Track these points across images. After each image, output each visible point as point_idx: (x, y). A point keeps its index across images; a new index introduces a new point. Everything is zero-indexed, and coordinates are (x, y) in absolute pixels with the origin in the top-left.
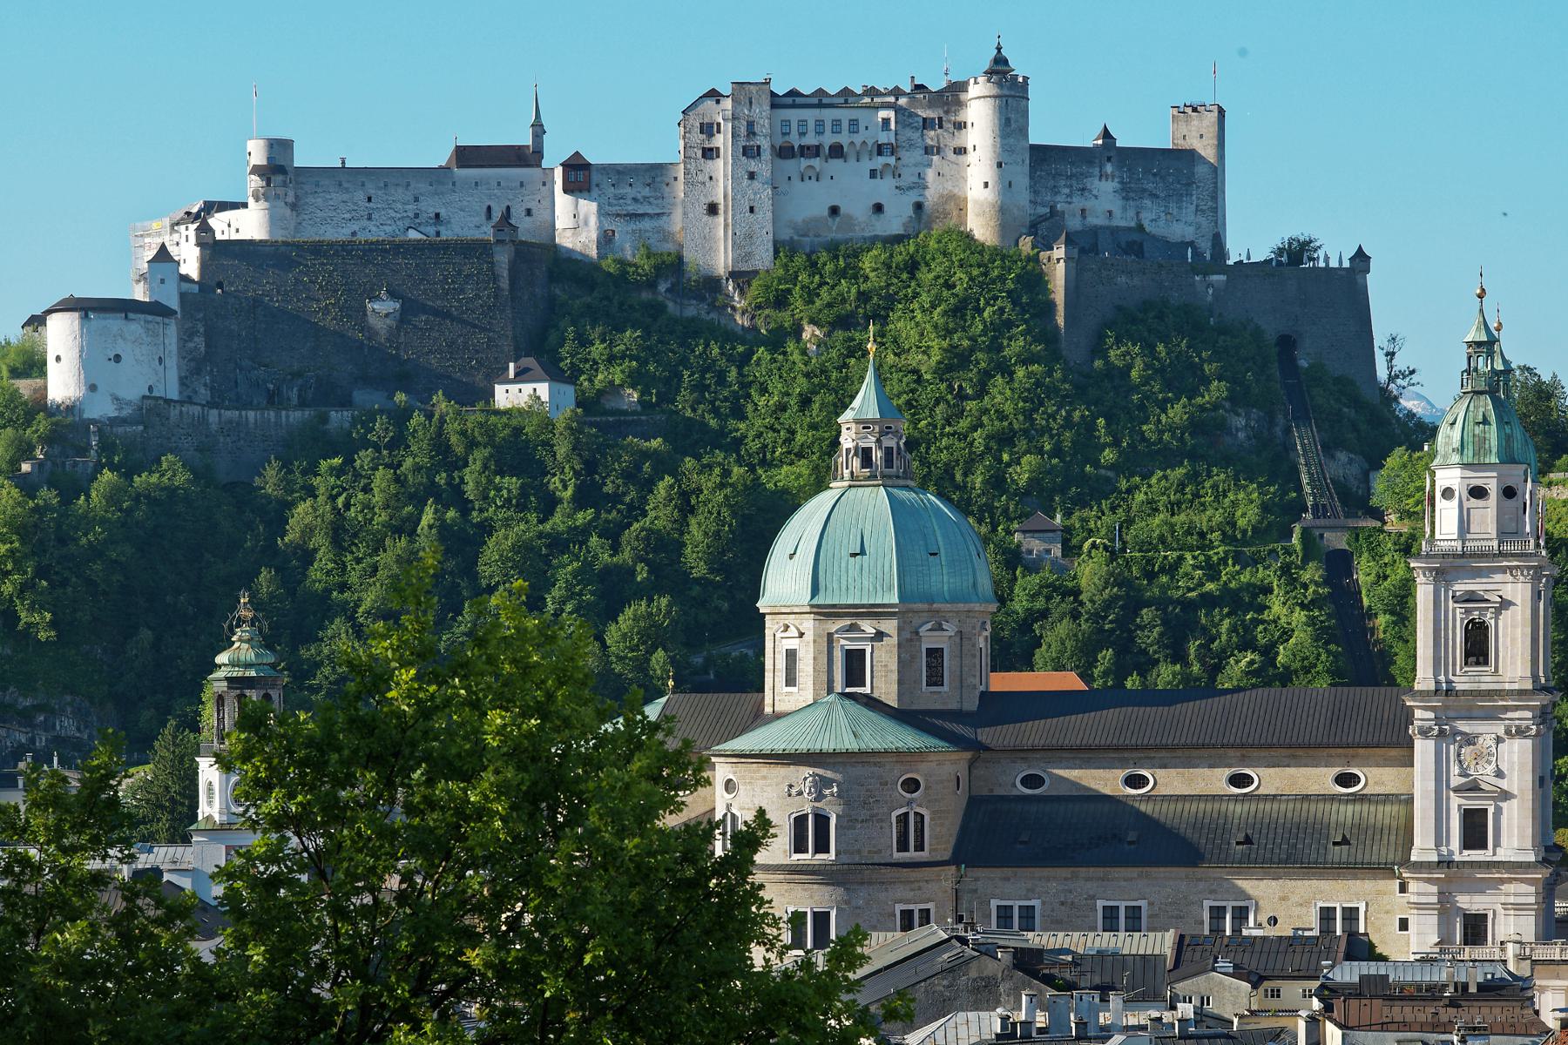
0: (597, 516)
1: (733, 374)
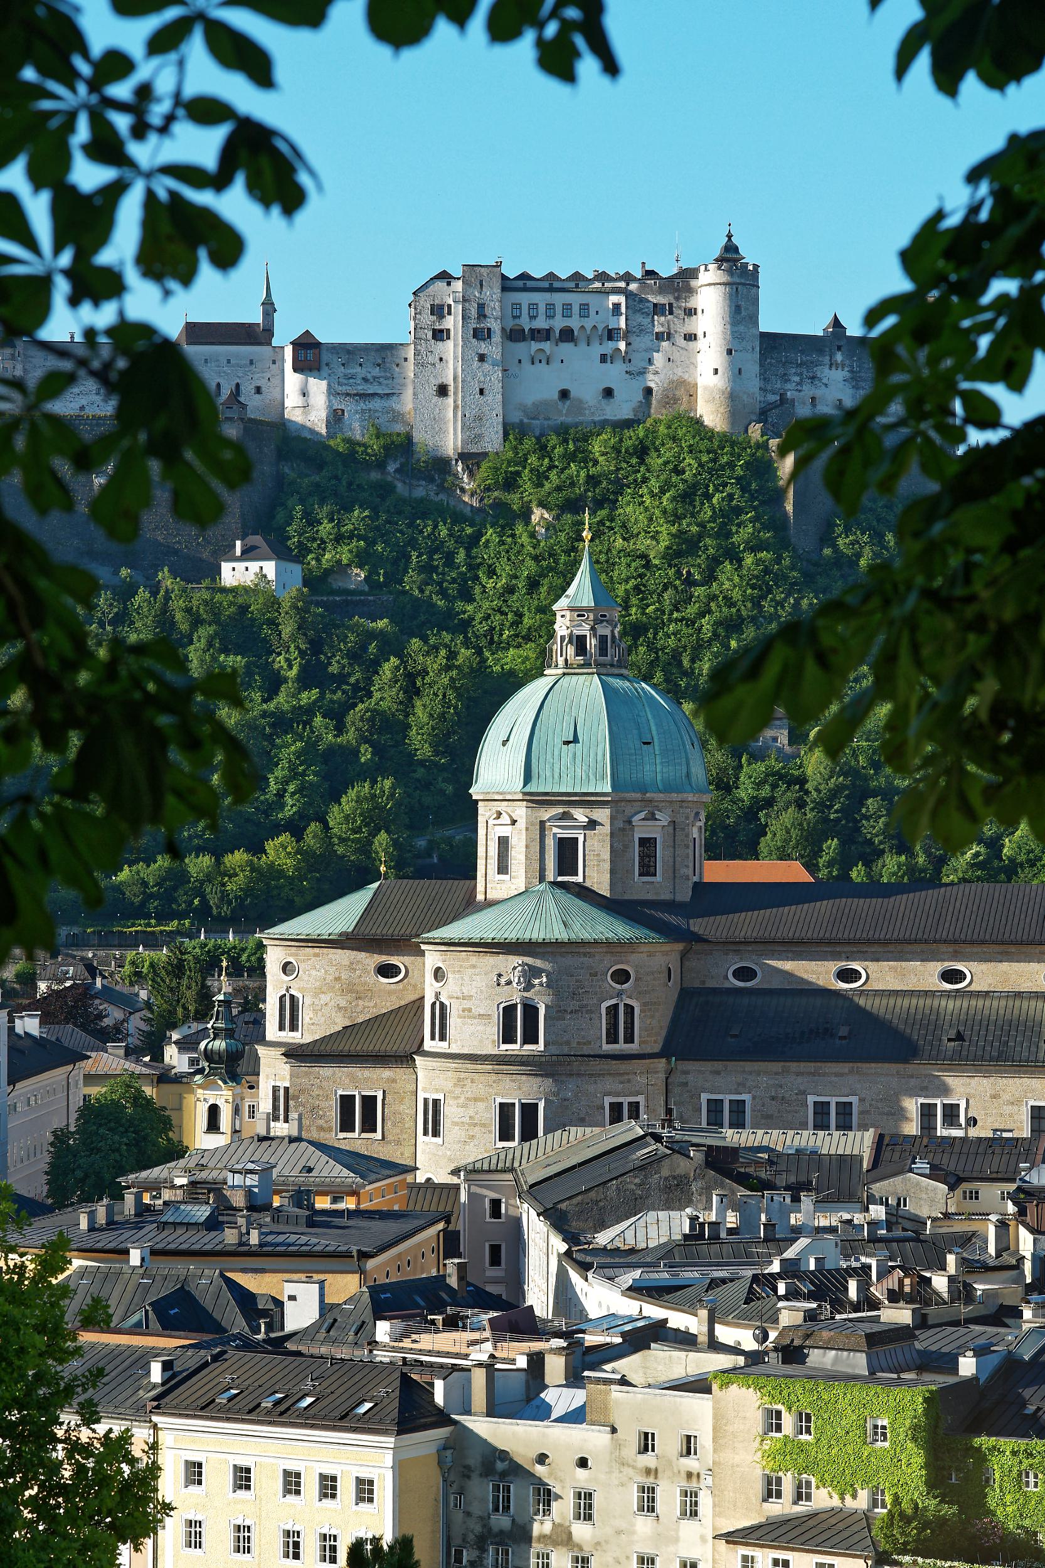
0: (322, 695)
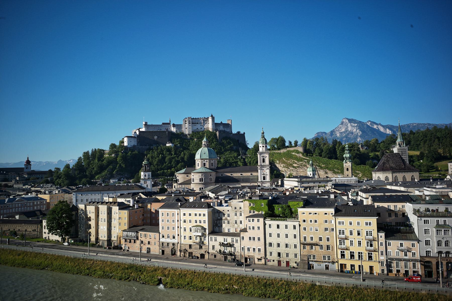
1: (188, 143)
